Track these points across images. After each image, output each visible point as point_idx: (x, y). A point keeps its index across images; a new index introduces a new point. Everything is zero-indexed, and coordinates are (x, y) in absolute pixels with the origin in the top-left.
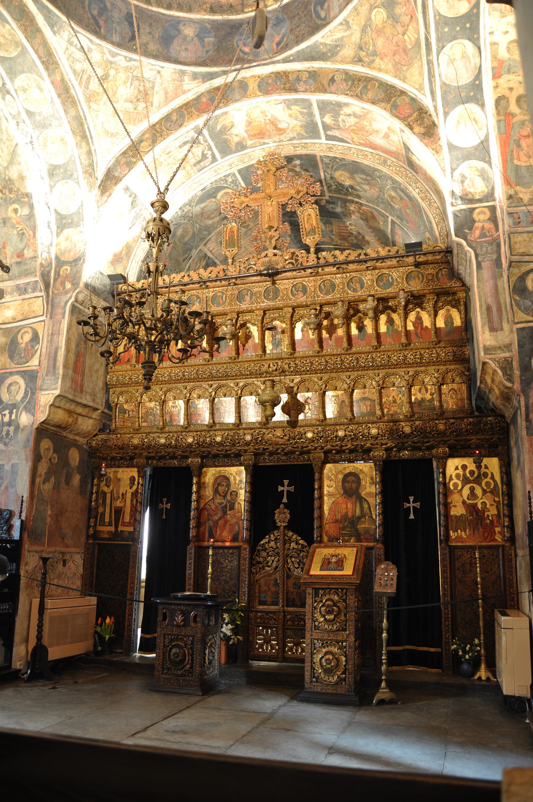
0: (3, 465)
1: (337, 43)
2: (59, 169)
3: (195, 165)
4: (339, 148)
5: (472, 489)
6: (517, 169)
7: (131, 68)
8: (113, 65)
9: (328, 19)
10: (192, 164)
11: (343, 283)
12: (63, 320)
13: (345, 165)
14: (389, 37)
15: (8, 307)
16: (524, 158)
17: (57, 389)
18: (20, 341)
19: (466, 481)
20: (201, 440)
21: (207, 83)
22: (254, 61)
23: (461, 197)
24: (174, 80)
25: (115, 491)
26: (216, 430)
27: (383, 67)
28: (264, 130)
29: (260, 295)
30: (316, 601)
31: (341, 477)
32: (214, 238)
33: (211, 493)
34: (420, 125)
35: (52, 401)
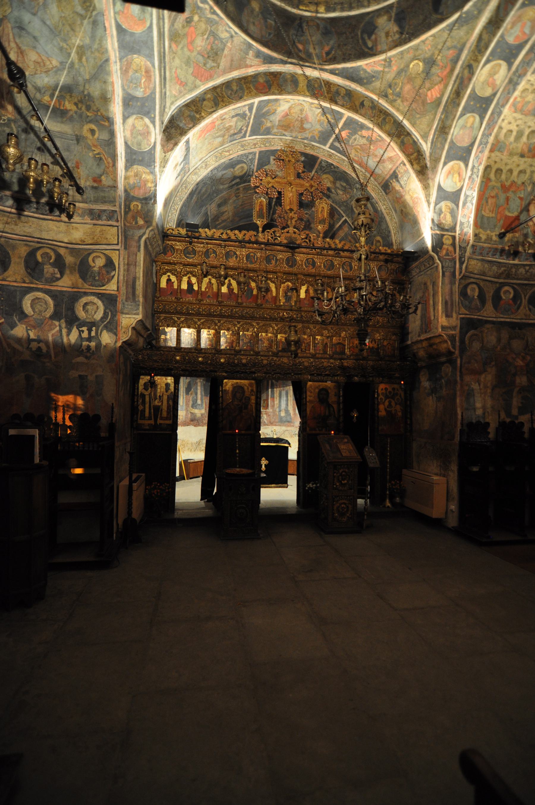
0: (87, 376)
1: (375, 75)
2: (137, 101)
3: (231, 136)
4: (336, 157)
6: (483, 216)
7: (211, 22)
8: (199, 11)
9: (374, 51)
10: (230, 134)
11: (339, 265)
12: (138, 253)
13: (336, 172)
14: (416, 87)
15: (77, 228)
16: (487, 211)
17: (138, 314)
18: (92, 264)
19: (387, 397)
20: (231, 361)
21: (266, 65)
22: (307, 62)
23: (437, 225)
24: (241, 50)
25: (152, 394)
26: (241, 355)
27: (401, 108)
28: (292, 125)
29: (283, 261)
30: (334, 473)
31: (317, 390)
32: (217, 200)
33: (231, 397)
34: (418, 163)
35: (134, 324)
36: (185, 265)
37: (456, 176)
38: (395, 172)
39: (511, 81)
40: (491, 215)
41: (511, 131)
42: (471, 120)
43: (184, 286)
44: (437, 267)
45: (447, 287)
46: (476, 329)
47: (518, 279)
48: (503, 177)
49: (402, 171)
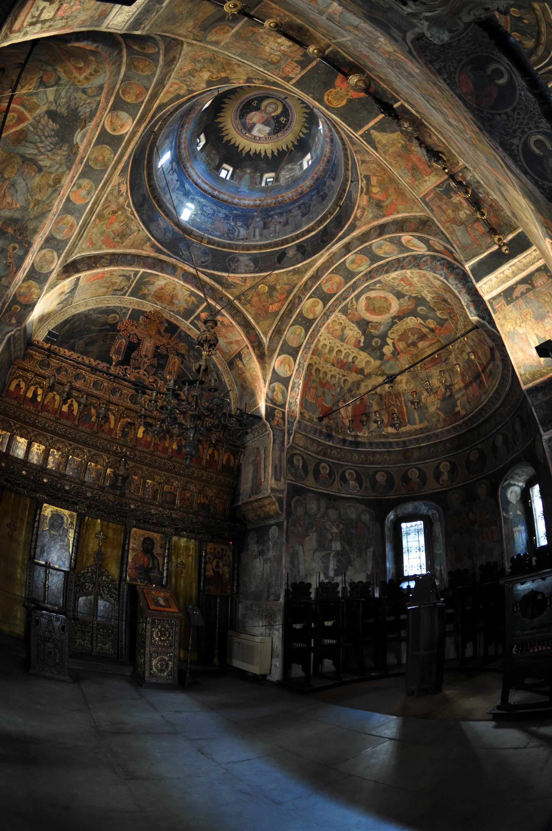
5: (218, 563)
6: (306, 401)
19: (215, 557)
31: (142, 539)
34: (259, 350)
36: (36, 375)
37: (287, 366)
38: (239, 353)
39: (325, 314)
40: (312, 401)
41: (326, 345)
42: (299, 330)
43: (30, 395)
44: (269, 434)
45: (277, 454)
46: (300, 495)
47: (332, 458)
48: (321, 375)
49: (245, 352)
